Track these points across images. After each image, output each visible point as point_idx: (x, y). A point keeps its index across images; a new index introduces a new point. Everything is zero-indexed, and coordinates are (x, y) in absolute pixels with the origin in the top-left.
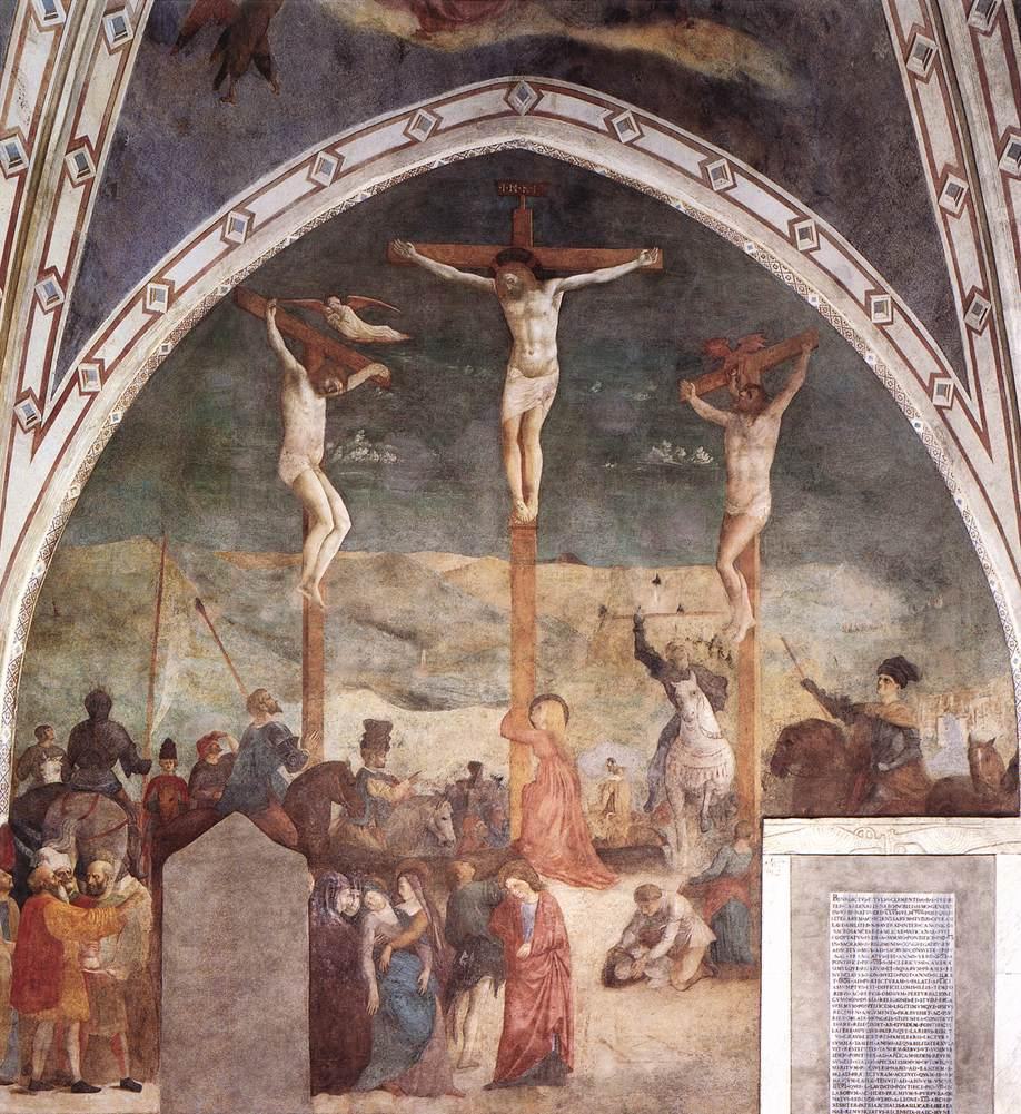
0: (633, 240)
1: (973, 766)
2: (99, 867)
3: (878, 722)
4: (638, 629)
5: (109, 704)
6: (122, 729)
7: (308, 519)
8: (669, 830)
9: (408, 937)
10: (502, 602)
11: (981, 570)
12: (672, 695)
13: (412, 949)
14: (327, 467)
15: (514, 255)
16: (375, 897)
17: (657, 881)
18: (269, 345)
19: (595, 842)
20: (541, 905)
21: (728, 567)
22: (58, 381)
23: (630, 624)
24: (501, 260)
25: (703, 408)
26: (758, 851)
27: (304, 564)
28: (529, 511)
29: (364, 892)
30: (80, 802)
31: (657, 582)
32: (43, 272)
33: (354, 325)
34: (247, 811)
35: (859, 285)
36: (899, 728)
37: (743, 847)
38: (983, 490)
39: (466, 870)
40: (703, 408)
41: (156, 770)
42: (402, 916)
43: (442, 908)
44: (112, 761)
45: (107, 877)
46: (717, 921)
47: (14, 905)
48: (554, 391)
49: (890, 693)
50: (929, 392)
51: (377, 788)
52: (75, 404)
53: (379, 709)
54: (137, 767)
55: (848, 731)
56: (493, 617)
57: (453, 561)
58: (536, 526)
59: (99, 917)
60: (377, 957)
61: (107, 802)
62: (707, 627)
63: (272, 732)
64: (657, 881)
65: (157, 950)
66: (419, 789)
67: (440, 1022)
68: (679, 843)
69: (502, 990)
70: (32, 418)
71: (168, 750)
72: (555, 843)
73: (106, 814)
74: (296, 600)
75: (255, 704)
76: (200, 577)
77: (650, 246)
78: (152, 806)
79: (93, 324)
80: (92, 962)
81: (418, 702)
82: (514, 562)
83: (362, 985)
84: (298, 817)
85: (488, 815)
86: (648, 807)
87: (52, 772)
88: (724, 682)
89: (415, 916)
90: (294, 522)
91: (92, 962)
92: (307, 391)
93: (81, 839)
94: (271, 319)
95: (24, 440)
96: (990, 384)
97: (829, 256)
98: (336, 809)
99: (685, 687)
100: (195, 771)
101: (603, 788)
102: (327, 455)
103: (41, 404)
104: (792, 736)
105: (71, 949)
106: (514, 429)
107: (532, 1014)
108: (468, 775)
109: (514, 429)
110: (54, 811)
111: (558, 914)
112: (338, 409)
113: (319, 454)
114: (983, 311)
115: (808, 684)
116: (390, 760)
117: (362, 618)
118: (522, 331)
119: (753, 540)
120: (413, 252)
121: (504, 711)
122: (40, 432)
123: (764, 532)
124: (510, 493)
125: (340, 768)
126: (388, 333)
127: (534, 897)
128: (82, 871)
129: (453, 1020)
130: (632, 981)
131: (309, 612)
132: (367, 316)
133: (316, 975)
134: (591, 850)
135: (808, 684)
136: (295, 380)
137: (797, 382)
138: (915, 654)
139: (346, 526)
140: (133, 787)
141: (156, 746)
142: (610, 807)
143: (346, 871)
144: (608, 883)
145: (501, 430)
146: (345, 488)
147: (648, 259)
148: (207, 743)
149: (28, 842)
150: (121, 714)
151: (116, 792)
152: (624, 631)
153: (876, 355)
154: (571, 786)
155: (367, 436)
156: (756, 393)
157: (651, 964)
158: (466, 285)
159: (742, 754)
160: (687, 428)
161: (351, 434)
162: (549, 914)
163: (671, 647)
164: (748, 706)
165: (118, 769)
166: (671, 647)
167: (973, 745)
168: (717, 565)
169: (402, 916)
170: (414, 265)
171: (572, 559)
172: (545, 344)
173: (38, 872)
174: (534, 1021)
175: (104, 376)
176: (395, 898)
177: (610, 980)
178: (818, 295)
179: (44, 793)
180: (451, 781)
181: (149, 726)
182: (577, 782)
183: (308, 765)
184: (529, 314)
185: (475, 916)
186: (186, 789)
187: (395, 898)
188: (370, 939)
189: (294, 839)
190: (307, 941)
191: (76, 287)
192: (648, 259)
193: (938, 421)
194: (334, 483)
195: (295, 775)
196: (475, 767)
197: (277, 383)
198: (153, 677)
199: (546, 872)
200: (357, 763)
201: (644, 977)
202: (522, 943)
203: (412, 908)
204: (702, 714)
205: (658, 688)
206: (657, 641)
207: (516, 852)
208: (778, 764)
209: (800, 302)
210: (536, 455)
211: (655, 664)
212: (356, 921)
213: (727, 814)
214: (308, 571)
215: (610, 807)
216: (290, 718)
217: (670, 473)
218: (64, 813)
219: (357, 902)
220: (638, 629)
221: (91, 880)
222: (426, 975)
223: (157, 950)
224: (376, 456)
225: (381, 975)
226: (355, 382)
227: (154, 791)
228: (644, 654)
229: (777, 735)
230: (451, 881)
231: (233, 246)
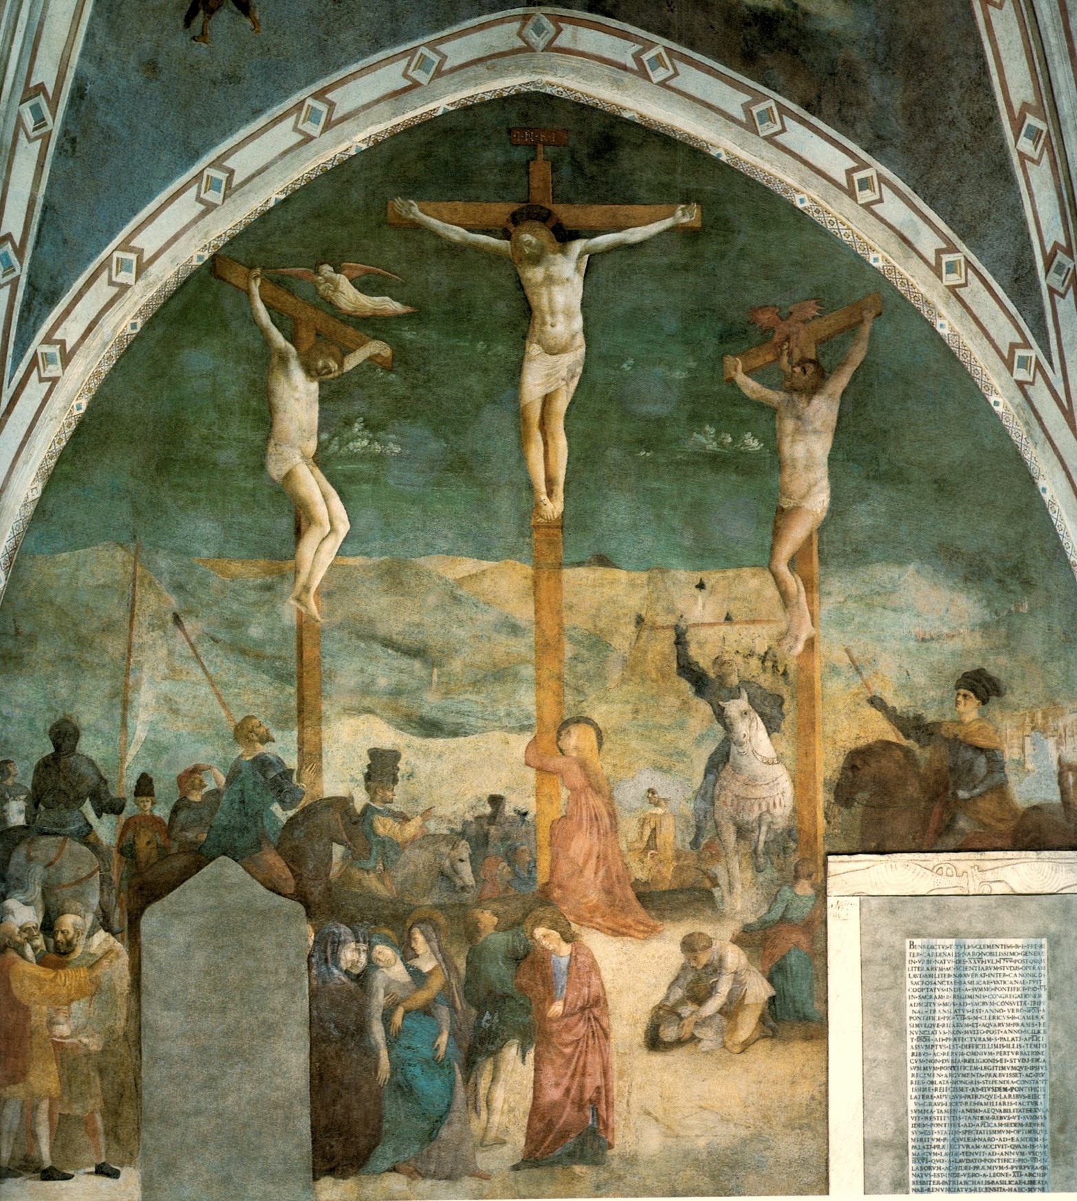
0: (668, 195)
3: (956, 744)
4: (680, 641)
6: (91, 763)
10: (524, 613)
12: (720, 715)
14: (321, 460)
15: (530, 214)
17: (707, 929)
21: (783, 568)
23: (671, 635)
25: (750, 386)
27: (297, 572)
31: (701, 586)
33: (349, 297)
36: (980, 750)
37: (804, 889)
41: (130, 808)
48: (579, 370)
49: (970, 710)
51: (384, 827)
53: (385, 736)
56: (514, 629)
58: (561, 524)
62: (760, 638)
63: (262, 764)
64: (707, 929)
71: (144, 786)
74: (288, 612)
75: (244, 732)
81: (430, 727)
86: (695, 844)
88: (779, 701)
92: (298, 375)
94: (255, 288)
98: (338, 850)
99: (735, 707)
100: (175, 811)
102: (321, 447)
104: (858, 759)
106: (535, 414)
108: (488, 810)
109: (535, 414)
113: (312, 446)
119: (810, 537)
120: (416, 211)
124: (531, 487)
125: (343, 804)
132: (364, 286)
135: (876, 702)
136: (284, 360)
137: (858, 354)
138: (997, 665)
139: (344, 527)
141: (131, 782)
144: (650, 932)
145: (520, 415)
147: (687, 216)
152: (663, 645)
155: (367, 425)
159: (802, 782)
161: (348, 423)
165: (88, 808)
171: (603, 561)
172: (569, 315)
175: (66, 359)
183: (305, 802)
184: (550, 280)
192: (687, 216)
194: (331, 479)
200: (361, 799)
205: (703, 708)
206: (702, 656)
208: (843, 792)
210: (561, 444)
211: (699, 681)
217: (716, 461)
220: (680, 641)
224: (377, 448)
226: (351, 362)
231: (210, 208)
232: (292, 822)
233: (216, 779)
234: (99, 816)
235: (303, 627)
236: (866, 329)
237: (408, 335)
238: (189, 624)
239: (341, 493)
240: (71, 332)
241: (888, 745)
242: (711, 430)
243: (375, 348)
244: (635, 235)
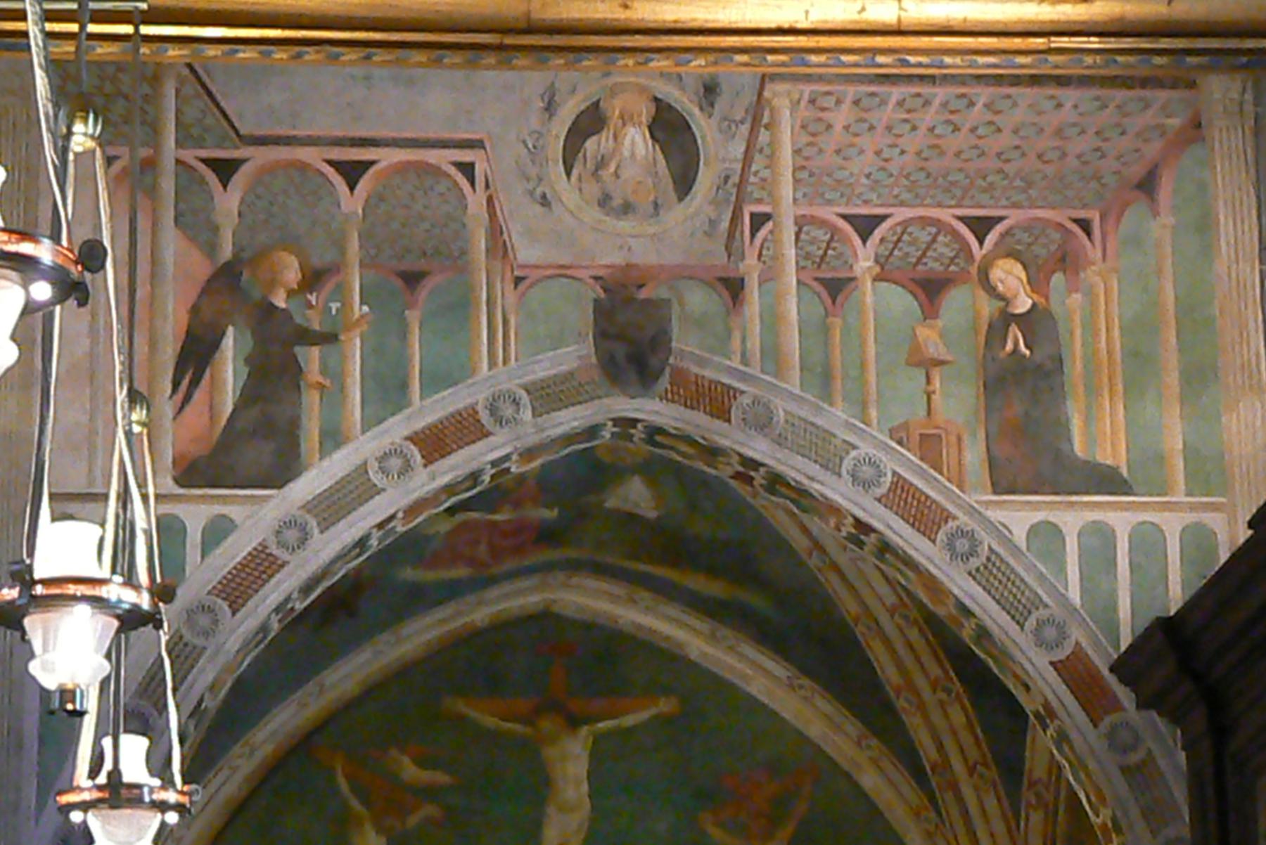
33: (410, 771)
48: (586, 825)
120: (460, 706)
126: (441, 778)
132: (422, 763)
147: (665, 706)
170: (462, 718)
192: (665, 706)
226: (413, 821)
243: (430, 810)
244: (629, 720)
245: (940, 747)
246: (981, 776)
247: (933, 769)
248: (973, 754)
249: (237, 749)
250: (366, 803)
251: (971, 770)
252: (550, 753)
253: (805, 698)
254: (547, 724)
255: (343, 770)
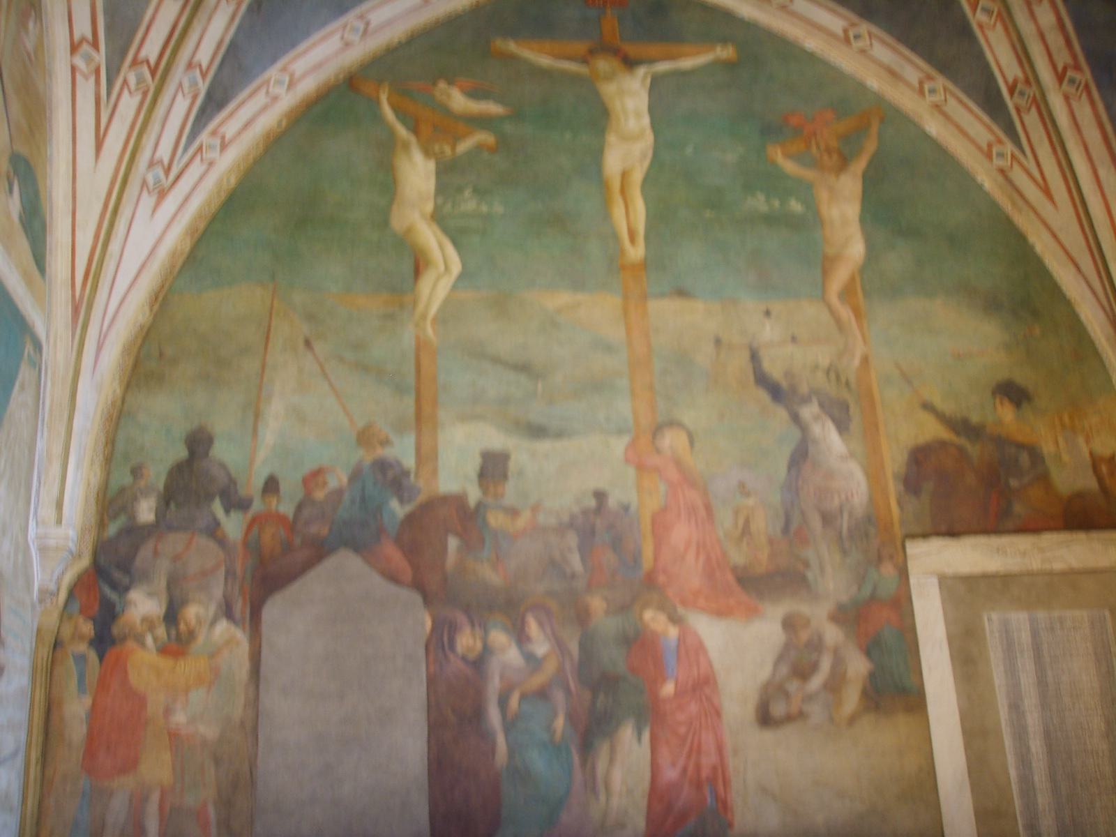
0: (708, 38)
1: (1100, 480)
2: (192, 612)
3: (1001, 442)
4: (754, 357)
5: (209, 441)
6: (223, 466)
7: (419, 265)
8: (809, 554)
9: (537, 681)
10: (615, 333)
11: (1068, 303)
12: (796, 418)
13: (543, 694)
14: (438, 218)
15: (604, 48)
16: (499, 637)
17: (805, 609)
18: (378, 118)
19: (734, 569)
20: (681, 640)
21: (834, 299)
22: (186, 149)
23: (746, 355)
24: (592, 52)
25: (789, 167)
26: (904, 574)
27: (415, 303)
28: (636, 252)
29: (486, 632)
30: (174, 542)
31: (768, 313)
32: (190, 66)
33: (458, 101)
34: (358, 547)
35: (912, 75)
36: (1021, 446)
37: (888, 570)
38: (1054, 236)
39: (597, 604)
40: (789, 167)
41: (257, 506)
42: (529, 657)
43: (574, 647)
44: (209, 498)
45: (199, 622)
46: (871, 648)
47: (93, 656)
48: (650, 154)
49: (1007, 413)
50: (989, 156)
51: (495, 520)
52: (196, 169)
53: (496, 440)
54: (235, 502)
55: (973, 450)
56: (609, 348)
57: (563, 298)
58: (644, 265)
59: (186, 668)
60: (503, 702)
61: (202, 541)
62: (823, 355)
63: (382, 466)
64: (805, 609)
65: (254, 702)
66: (541, 519)
67: (578, 776)
68: (822, 570)
69: (646, 736)
70: (157, 181)
71: (271, 485)
72: (691, 574)
73: (203, 554)
74: (408, 338)
75: (365, 437)
76: (310, 318)
77: (724, 41)
78: (251, 544)
79: (221, 105)
80: (180, 718)
81: (537, 431)
82: (626, 298)
83: (486, 737)
84: (412, 550)
85: (617, 544)
86: (786, 529)
87: (146, 512)
88: (845, 407)
89: (545, 658)
90: (407, 266)
91: (180, 718)
92: (418, 156)
93: (173, 583)
94: (384, 98)
95: (148, 201)
96: (1044, 151)
97: (882, 53)
98: (453, 543)
99: (809, 412)
100: (300, 508)
101: (736, 513)
102: (437, 209)
103: (167, 171)
104: (920, 456)
105: (155, 703)
106: (616, 184)
107: (681, 762)
108: (592, 503)
109: (616, 184)
110: (145, 552)
111: (700, 648)
112: (447, 172)
113: (429, 207)
114: (1026, 97)
115: (928, 407)
116: (510, 492)
117: (478, 353)
118: (616, 106)
119: (852, 279)
121: (626, 439)
122: (162, 194)
123: (863, 269)
124: (616, 237)
125: (458, 501)
127: (673, 632)
128: (172, 616)
129: (594, 768)
130: (789, 718)
131: (421, 346)
132: (474, 94)
133: (435, 726)
134: (730, 578)
135: (928, 407)
136: (406, 147)
137: (871, 146)
138: (1023, 376)
139: (456, 268)
140: (233, 526)
141: (258, 482)
142: (746, 531)
143: (467, 610)
144: (752, 613)
145: (603, 185)
146: (457, 236)
147: (725, 52)
148: (314, 478)
149: (114, 586)
150: (225, 452)
151: (214, 531)
152: (739, 362)
153: (933, 127)
154: (702, 512)
155: (476, 191)
156: (835, 157)
157: (809, 698)
158: (564, 74)
159: (874, 474)
160: (774, 182)
161: (460, 190)
162: (692, 649)
163: (788, 374)
164: (872, 430)
165: (217, 507)
166: (788, 374)
167: (1095, 462)
168: (824, 298)
169: (529, 657)
170: (512, 58)
171: (681, 293)
172: (638, 115)
173: (122, 621)
174: (685, 770)
175: (224, 146)
176: (521, 637)
177: (765, 719)
178: (874, 82)
179: (135, 534)
180: (576, 509)
181: (252, 461)
182: (708, 508)
183: (421, 498)
185: (613, 658)
186: (291, 526)
187: (521, 637)
188: (494, 686)
189: (408, 574)
190: (423, 689)
191: (216, 75)
192: (725, 52)
193: (1000, 179)
194: (446, 231)
195: (408, 508)
196: (600, 496)
197: (387, 150)
198: (257, 415)
199: (684, 603)
200: (474, 495)
201: (801, 715)
202: (664, 680)
203: (541, 647)
204: (830, 440)
205: (781, 413)
206: (774, 368)
207: (650, 581)
208: (911, 483)
209: (861, 87)
211: (776, 392)
212: (479, 664)
213: (867, 535)
214: (421, 307)
215: (746, 531)
216: (403, 451)
217: (770, 220)
218: (156, 553)
219: (479, 645)
220: (754, 357)
221: (182, 627)
222: (560, 723)
223: (254, 702)
224: (484, 208)
225: (509, 726)
226: (464, 147)
227: (255, 530)
228: (762, 379)
229: (906, 456)
230: (582, 617)
231: (347, 45)
232: (410, 519)
233: (338, 479)
234: (227, 511)
235: (421, 346)
236: (875, 128)
237: (508, 128)
238: (318, 347)
239: (455, 243)
240: (230, 129)
241: (943, 444)
242: (761, 197)
243: (483, 137)
244: (687, 63)
245: (1023, 56)
246: (1072, 81)
247: (1012, 90)
248: (1063, 58)
249: (273, 72)
250: (415, 130)
251: (1060, 78)
252: (608, 90)
253: (863, 51)
254: (603, 64)
255: (388, 99)
